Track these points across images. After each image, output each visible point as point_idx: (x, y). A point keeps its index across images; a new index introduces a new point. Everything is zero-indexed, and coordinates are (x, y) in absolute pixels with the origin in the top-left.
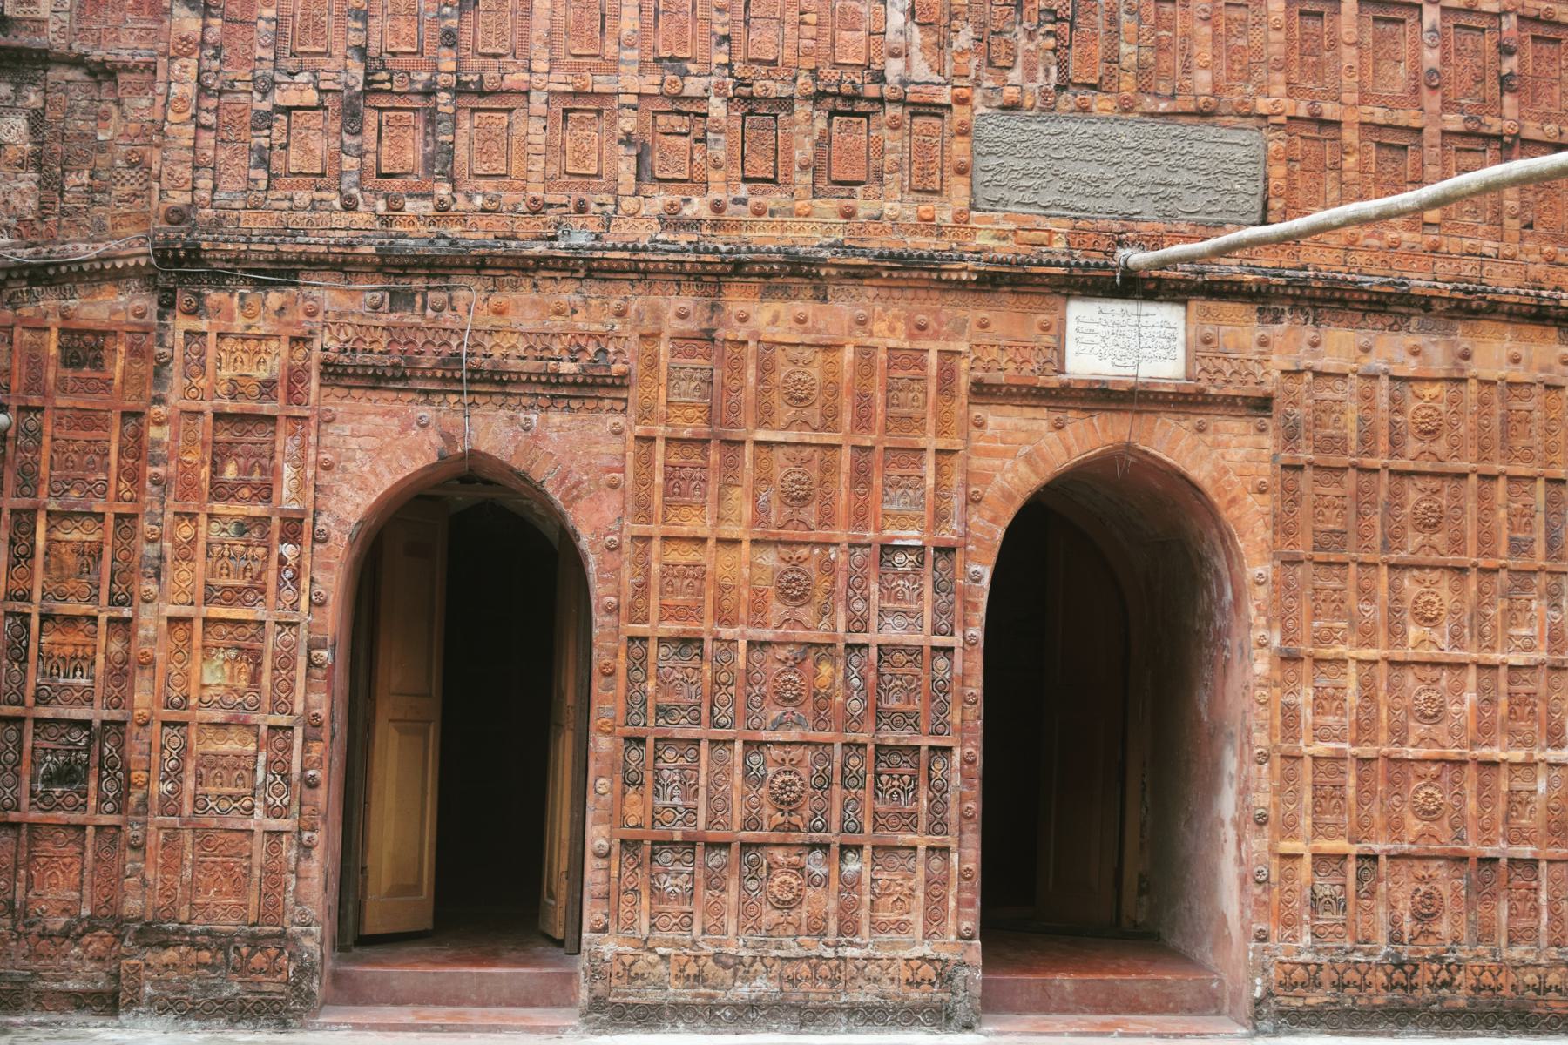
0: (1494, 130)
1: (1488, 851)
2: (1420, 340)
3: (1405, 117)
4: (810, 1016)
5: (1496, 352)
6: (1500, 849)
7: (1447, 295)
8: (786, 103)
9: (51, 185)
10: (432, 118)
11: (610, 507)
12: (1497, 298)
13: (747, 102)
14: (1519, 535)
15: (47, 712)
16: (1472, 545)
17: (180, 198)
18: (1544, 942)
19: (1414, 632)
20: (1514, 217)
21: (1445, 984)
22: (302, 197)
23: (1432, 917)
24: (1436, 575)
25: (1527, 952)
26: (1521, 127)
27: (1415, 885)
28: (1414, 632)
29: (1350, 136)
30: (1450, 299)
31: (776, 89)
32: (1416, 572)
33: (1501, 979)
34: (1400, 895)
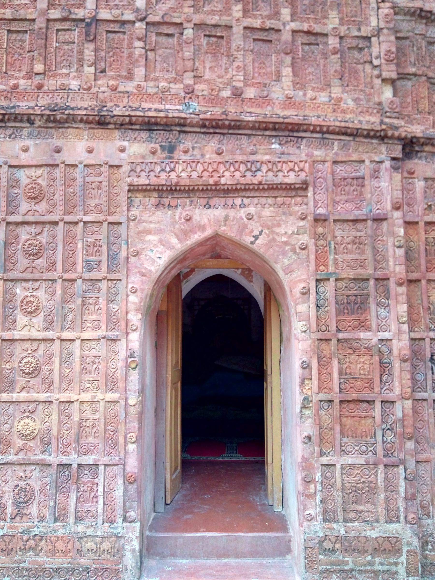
0: (80, 16)
1: (64, 460)
2: (28, 142)
5: (77, 147)
6: (73, 458)
7: (39, 112)
12: (71, 112)
14: (92, 258)
16: (59, 266)
18: (100, 521)
19: (22, 319)
20: (90, 66)
21: (30, 549)
24: (37, 284)
25: (88, 527)
26: (97, 13)
27: (16, 483)
28: (22, 319)
30: (42, 115)
32: (24, 284)
33: (70, 546)
34: (6, 489)
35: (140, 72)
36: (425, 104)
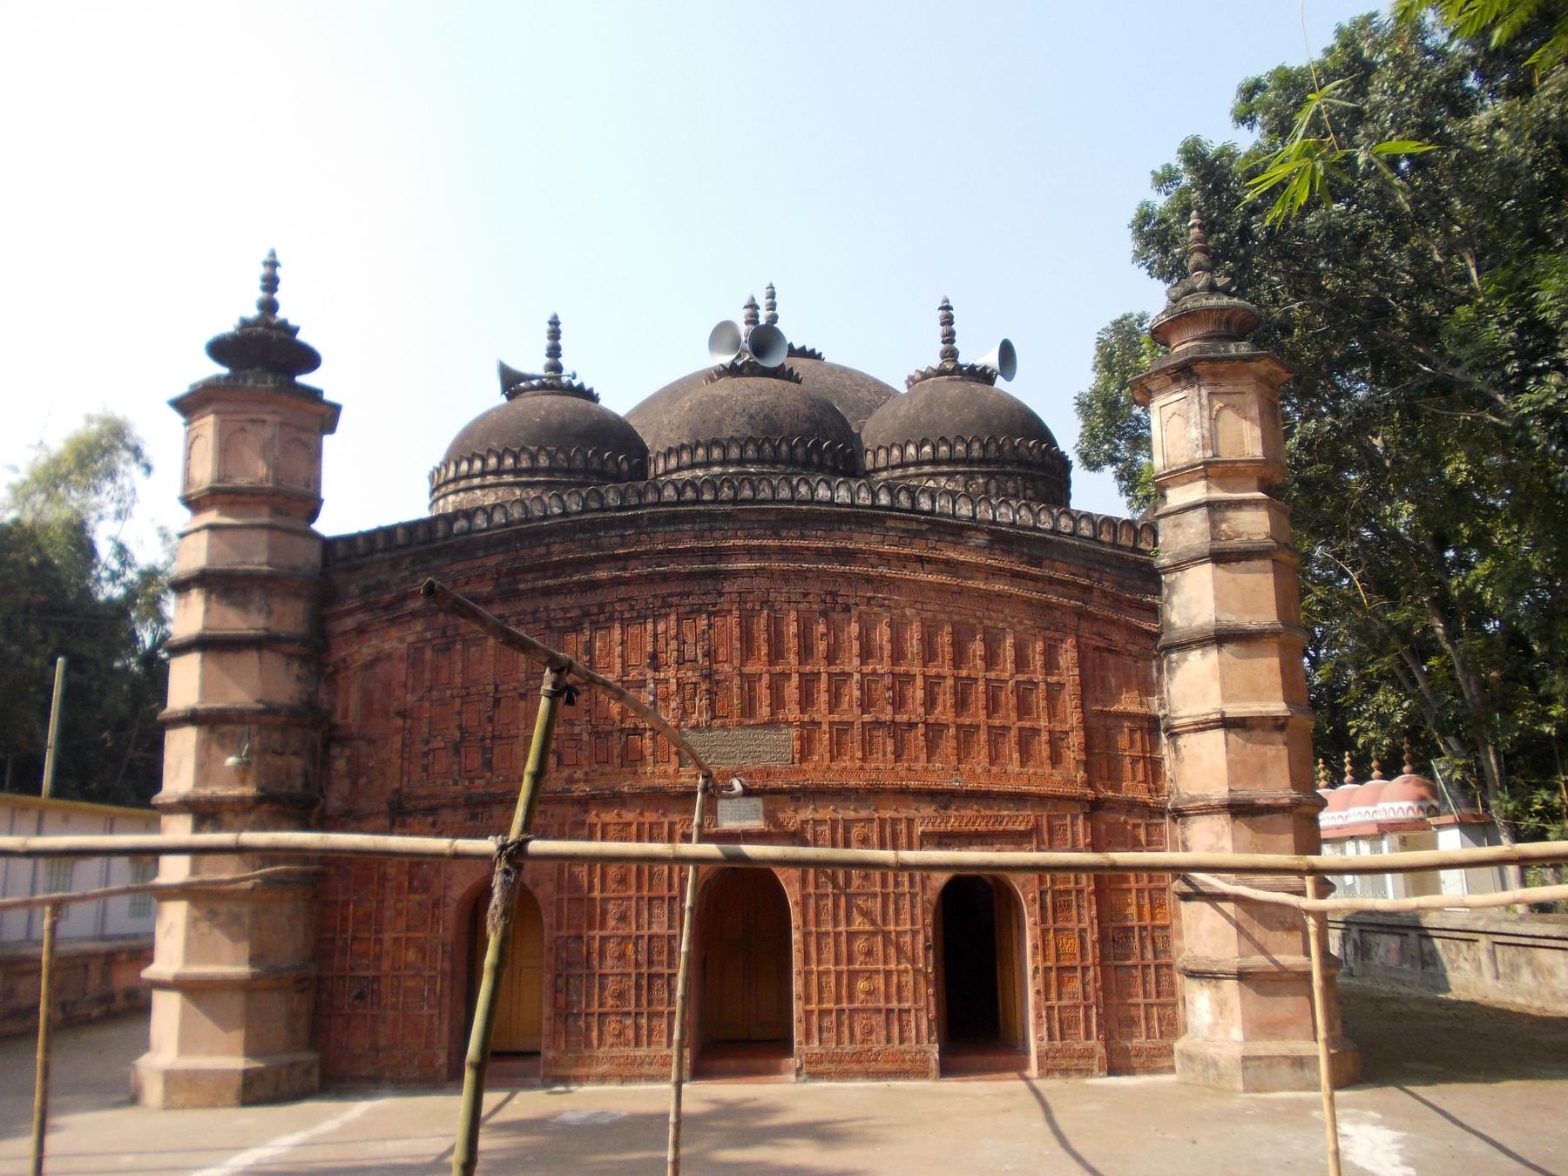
3: (845, 718)
8: (611, 733)
9: (355, 783)
10: (484, 750)
11: (549, 888)
13: (596, 734)
15: (354, 974)
17: (397, 785)
22: (439, 782)
23: (870, 1033)
29: (825, 727)
31: (609, 728)
35: (923, 757)
36: (1105, 773)
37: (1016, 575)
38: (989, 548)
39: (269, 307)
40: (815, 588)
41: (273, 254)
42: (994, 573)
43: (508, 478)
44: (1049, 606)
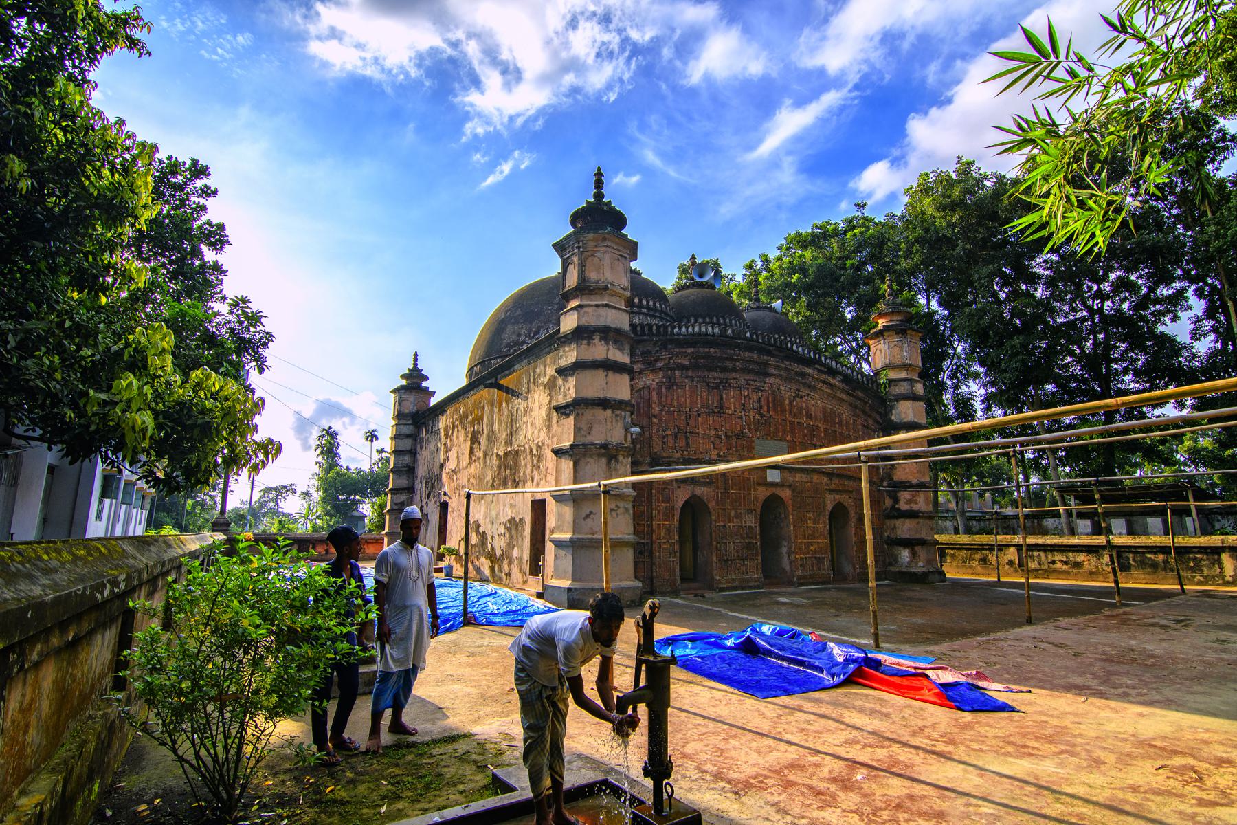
4: (743, 588)
5: (816, 478)
10: (687, 438)
37: (849, 394)
38: (842, 381)
39: (599, 196)
40: (794, 387)
41: (599, 170)
42: (844, 391)
43: (644, 310)
44: (856, 407)
